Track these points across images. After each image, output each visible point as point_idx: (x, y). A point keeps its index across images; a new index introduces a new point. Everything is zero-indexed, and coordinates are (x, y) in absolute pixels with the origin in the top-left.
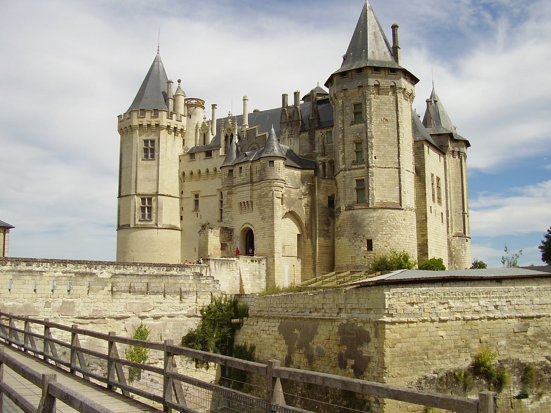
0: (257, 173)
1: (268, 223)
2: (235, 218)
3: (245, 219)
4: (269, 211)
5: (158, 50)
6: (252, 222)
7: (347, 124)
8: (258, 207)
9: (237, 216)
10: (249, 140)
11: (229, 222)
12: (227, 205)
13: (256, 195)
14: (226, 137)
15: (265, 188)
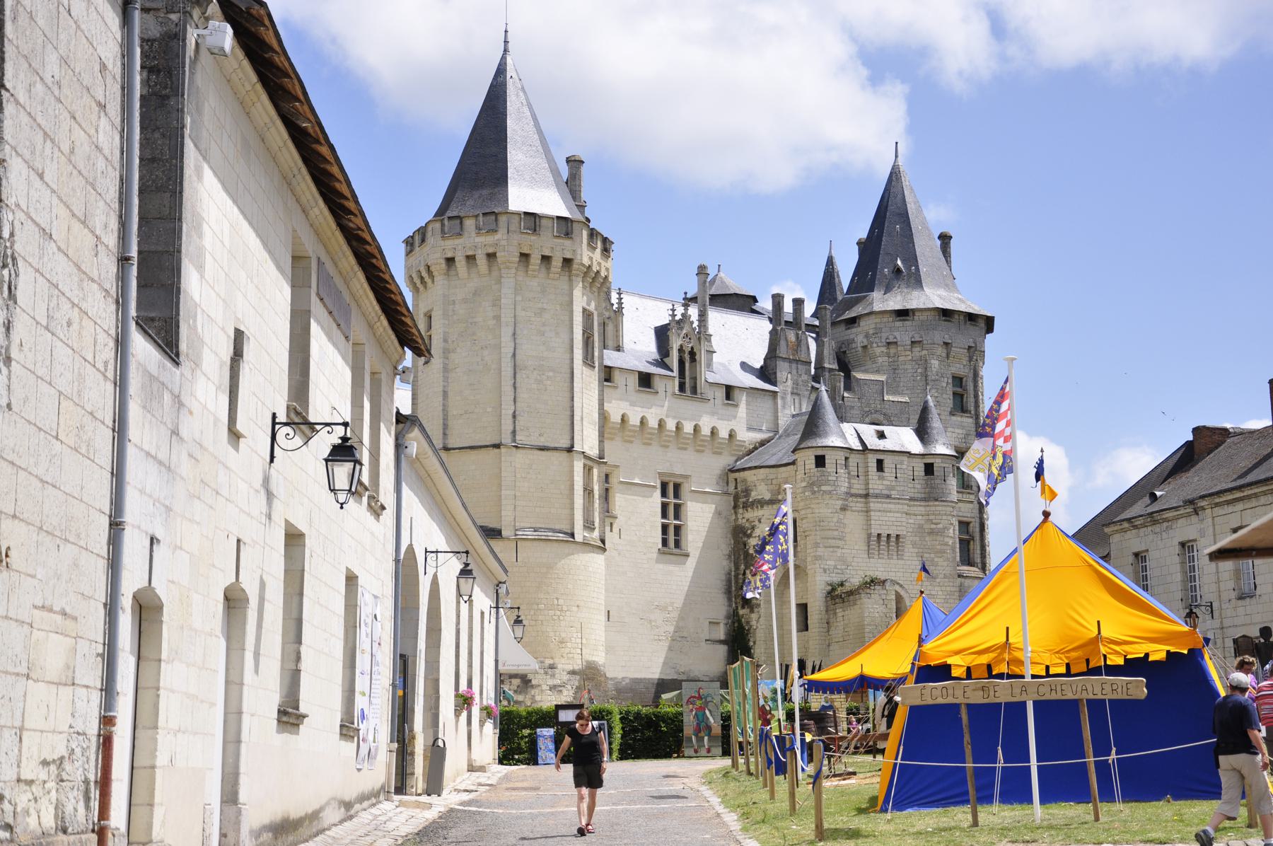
0: (913, 480)
1: (943, 588)
2: (853, 564)
3: (883, 569)
4: (945, 564)
5: (506, 42)
6: (902, 578)
7: (944, 411)
8: (916, 550)
9: (860, 560)
10: (864, 401)
11: (836, 571)
12: (836, 533)
13: (912, 526)
14: (681, 350)
15: (944, 517)
